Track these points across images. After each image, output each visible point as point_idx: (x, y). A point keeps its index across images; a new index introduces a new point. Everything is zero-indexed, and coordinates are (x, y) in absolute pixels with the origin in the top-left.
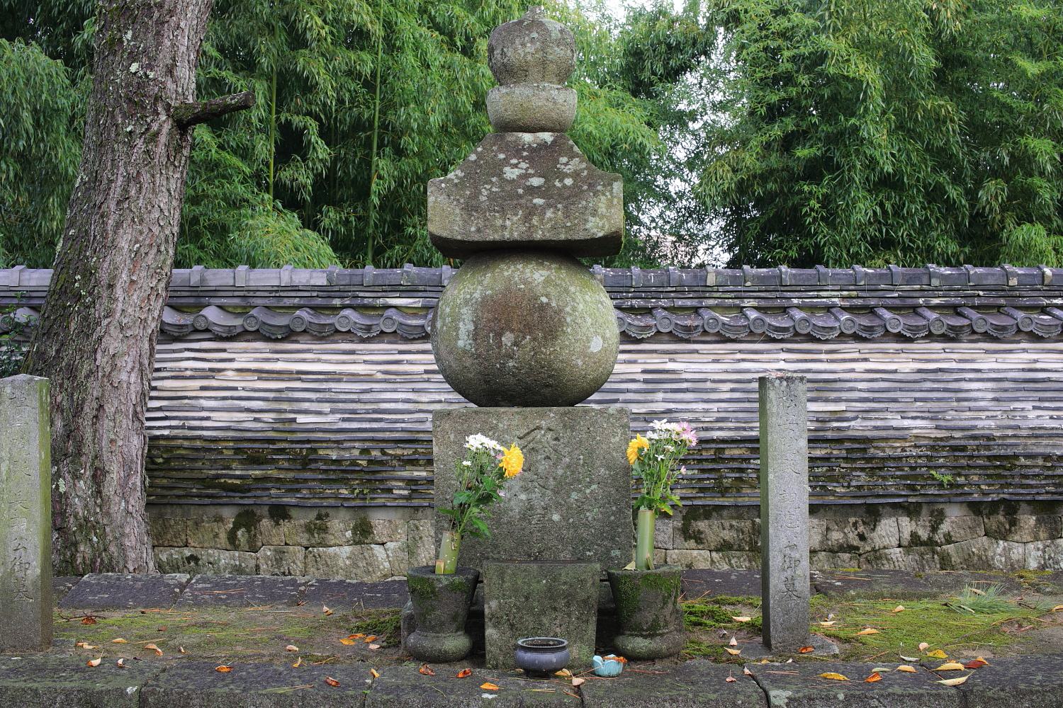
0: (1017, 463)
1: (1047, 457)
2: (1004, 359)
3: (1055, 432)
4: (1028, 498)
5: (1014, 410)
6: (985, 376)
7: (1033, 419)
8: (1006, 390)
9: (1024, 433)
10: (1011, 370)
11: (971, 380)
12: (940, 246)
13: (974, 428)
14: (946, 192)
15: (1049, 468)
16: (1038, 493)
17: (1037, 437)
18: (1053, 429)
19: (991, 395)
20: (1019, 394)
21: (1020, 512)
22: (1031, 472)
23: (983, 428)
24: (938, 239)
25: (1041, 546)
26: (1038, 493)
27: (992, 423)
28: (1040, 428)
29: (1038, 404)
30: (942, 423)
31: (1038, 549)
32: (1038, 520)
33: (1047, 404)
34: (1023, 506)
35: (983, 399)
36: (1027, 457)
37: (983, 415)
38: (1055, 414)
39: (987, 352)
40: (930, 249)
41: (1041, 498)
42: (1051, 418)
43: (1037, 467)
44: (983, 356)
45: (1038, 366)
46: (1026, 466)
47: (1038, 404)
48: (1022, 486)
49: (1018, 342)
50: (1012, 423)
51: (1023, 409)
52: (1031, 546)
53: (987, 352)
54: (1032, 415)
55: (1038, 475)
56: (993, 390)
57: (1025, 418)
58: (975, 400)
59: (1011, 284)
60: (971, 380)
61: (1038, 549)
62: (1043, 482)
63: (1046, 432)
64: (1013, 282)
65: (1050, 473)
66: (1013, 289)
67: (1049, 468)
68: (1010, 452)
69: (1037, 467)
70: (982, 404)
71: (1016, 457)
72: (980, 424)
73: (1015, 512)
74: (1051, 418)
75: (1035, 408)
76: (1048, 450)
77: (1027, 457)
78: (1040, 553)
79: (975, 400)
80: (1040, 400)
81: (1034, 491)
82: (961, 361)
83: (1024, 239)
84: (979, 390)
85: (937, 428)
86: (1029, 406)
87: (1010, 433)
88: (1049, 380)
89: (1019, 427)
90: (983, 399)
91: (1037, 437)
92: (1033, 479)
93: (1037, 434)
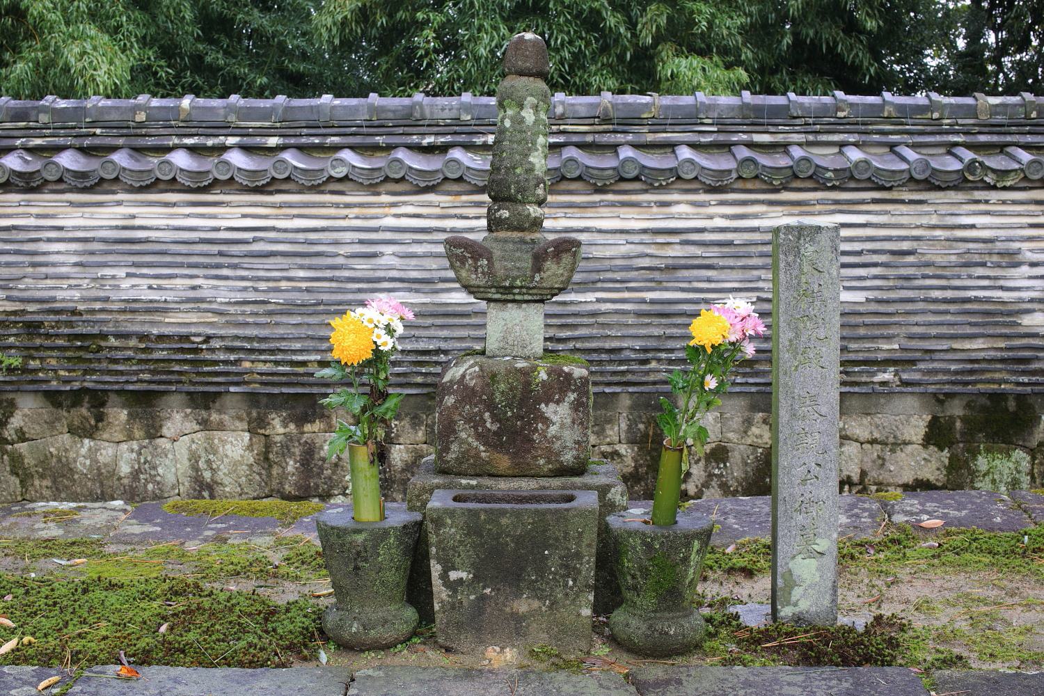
0: (103, 344)
1: (143, 337)
2: (92, 213)
3: (156, 305)
4: (116, 387)
5: (103, 278)
6: (70, 235)
7: (127, 289)
8: (92, 253)
9: (115, 307)
10: (101, 227)
11: (49, 240)
12: (595, 81)
13: (53, 300)
14: (604, 19)
15: (144, 350)
16: (127, 382)
17: (133, 311)
18: (151, 301)
19: (75, 259)
20: (110, 258)
21: (109, 404)
22: (119, 355)
23: (63, 300)
24: (595, 74)
25: (136, 447)
26: (127, 382)
27: (77, 294)
28: (135, 301)
29: (133, 270)
30: (15, 294)
31: (132, 451)
32: (130, 414)
33: (145, 271)
34: (113, 397)
35: (63, 264)
36: (118, 336)
37: (65, 284)
38: (154, 282)
39: (72, 204)
40: (589, 84)
41: (131, 387)
42: (150, 287)
43: (130, 348)
44: (69, 209)
45: (137, 222)
46: (116, 348)
47: (133, 270)
48: (110, 372)
49: (114, 193)
50: (102, 294)
51: (113, 277)
52: (124, 446)
53: (72, 204)
54: (126, 284)
55: (129, 359)
56: (76, 253)
57: (117, 287)
58: (54, 265)
59: (138, 119)
60: (49, 240)
61: (132, 451)
62: (134, 368)
63: (145, 305)
64: (141, 117)
65: (143, 356)
66: (141, 125)
67: (144, 350)
68: (96, 330)
69: (130, 348)
70: (63, 270)
71: (104, 336)
72: (60, 295)
73: (103, 404)
74: (150, 287)
75: (129, 275)
76: (146, 329)
77: (118, 336)
78: (134, 455)
79: (54, 265)
80: (135, 265)
81: (123, 379)
82: (38, 216)
83: (672, 71)
84: (58, 253)
85: (9, 299)
86: (121, 272)
87: (98, 306)
88: (147, 241)
89: (107, 299)
90: (63, 264)
91: (133, 311)
92: (123, 364)
93: (132, 308)
